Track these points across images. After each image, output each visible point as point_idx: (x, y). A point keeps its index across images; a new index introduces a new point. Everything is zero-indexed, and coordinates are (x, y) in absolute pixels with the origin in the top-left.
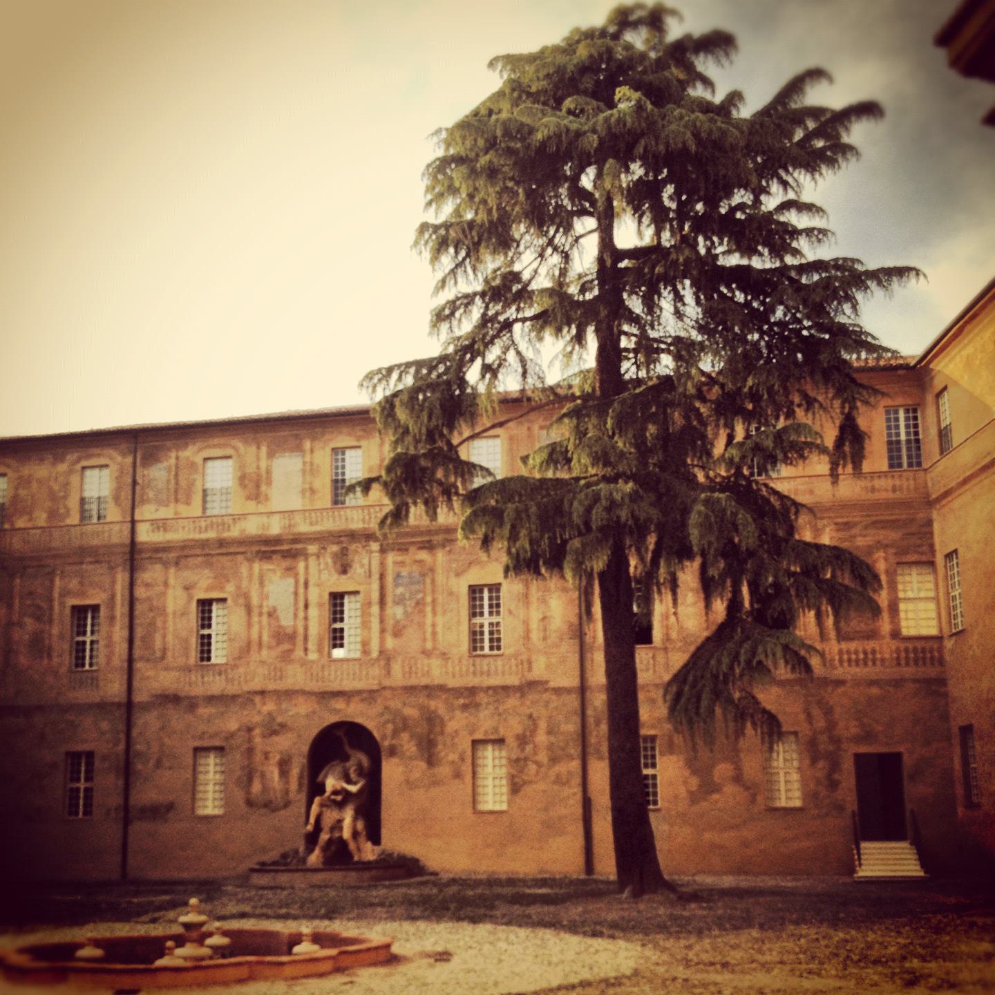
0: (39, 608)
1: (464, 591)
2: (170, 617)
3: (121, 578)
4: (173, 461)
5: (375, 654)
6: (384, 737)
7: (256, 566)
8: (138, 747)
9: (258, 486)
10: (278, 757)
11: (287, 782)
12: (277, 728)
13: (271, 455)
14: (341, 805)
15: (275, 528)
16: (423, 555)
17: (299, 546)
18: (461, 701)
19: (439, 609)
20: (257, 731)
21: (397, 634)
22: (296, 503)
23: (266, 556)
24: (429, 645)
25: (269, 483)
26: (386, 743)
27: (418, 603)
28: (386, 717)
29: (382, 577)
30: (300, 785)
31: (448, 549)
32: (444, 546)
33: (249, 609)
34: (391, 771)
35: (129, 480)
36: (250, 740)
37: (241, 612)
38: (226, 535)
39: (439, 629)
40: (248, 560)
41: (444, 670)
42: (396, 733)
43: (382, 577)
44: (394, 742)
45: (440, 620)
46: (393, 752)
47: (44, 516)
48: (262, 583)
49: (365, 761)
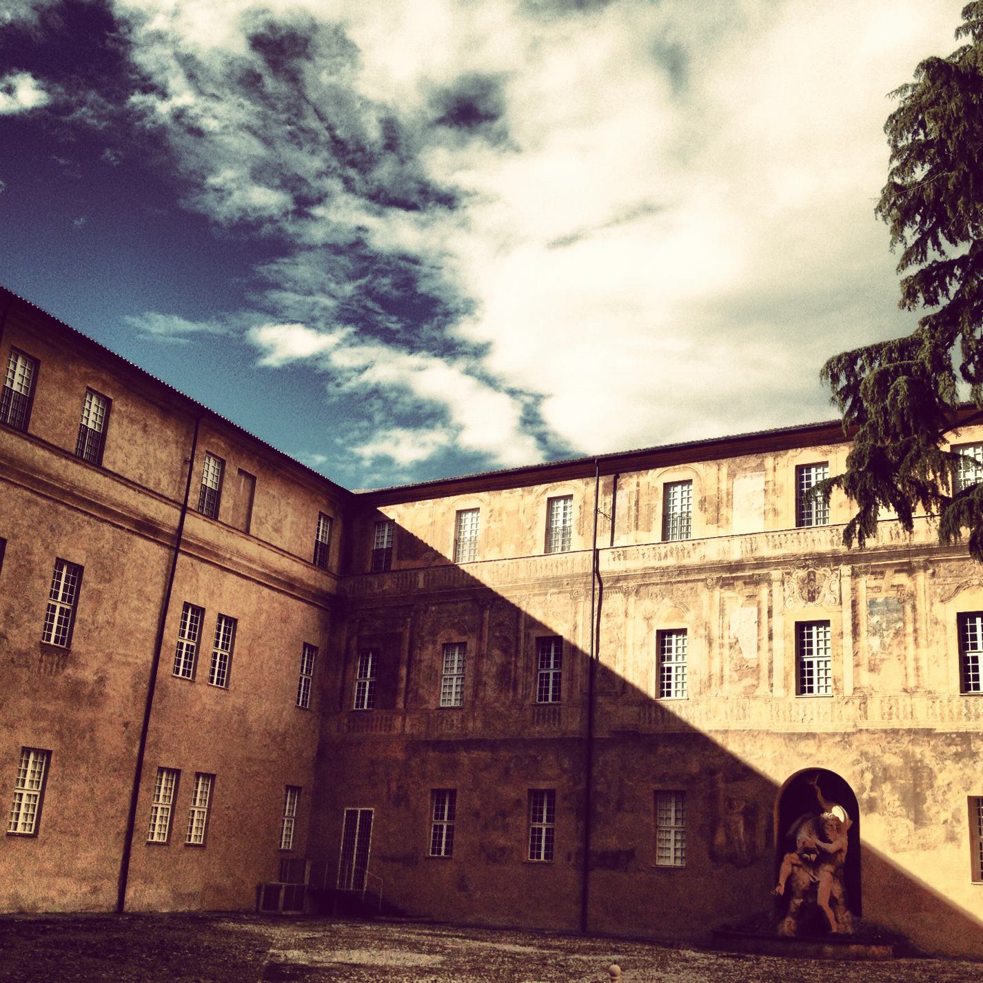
0: (506, 639)
1: (953, 620)
2: (630, 649)
3: (585, 607)
4: (634, 488)
5: (848, 691)
6: (862, 789)
7: (717, 592)
8: (599, 787)
9: (718, 509)
13: (732, 475)
14: (815, 866)
15: (736, 553)
16: (902, 579)
17: (764, 571)
18: (953, 749)
19: (922, 641)
20: (720, 775)
21: (872, 669)
22: (758, 525)
23: (726, 583)
24: (912, 683)
25: (730, 504)
26: (865, 796)
27: (897, 633)
28: (865, 764)
29: (854, 604)
31: (931, 571)
32: (926, 569)
33: (710, 644)
35: (593, 509)
37: (703, 643)
38: (686, 562)
39: (923, 663)
40: (707, 586)
41: (931, 711)
42: (875, 784)
43: (854, 604)
44: (873, 794)
45: (923, 653)
46: (872, 806)
47: (513, 547)
48: (722, 611)
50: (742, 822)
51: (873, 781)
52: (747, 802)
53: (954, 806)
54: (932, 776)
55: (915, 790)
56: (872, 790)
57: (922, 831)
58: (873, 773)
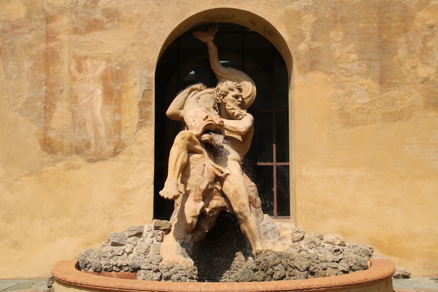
10: (100, 70)
11: (119, 111)
12: (98, 15)
20: (64, 21)
26: (302, 47)
30: (143, 116)
36: (50, 37)
42: (319, 29)
44: (316, 45)
46: (313, 65)
49: (249, 88)
50: (99, 92)
52: (109, 61)
54: (407, 17)
56: (313, 40)
57: (395, 93)
58: (316, 14)
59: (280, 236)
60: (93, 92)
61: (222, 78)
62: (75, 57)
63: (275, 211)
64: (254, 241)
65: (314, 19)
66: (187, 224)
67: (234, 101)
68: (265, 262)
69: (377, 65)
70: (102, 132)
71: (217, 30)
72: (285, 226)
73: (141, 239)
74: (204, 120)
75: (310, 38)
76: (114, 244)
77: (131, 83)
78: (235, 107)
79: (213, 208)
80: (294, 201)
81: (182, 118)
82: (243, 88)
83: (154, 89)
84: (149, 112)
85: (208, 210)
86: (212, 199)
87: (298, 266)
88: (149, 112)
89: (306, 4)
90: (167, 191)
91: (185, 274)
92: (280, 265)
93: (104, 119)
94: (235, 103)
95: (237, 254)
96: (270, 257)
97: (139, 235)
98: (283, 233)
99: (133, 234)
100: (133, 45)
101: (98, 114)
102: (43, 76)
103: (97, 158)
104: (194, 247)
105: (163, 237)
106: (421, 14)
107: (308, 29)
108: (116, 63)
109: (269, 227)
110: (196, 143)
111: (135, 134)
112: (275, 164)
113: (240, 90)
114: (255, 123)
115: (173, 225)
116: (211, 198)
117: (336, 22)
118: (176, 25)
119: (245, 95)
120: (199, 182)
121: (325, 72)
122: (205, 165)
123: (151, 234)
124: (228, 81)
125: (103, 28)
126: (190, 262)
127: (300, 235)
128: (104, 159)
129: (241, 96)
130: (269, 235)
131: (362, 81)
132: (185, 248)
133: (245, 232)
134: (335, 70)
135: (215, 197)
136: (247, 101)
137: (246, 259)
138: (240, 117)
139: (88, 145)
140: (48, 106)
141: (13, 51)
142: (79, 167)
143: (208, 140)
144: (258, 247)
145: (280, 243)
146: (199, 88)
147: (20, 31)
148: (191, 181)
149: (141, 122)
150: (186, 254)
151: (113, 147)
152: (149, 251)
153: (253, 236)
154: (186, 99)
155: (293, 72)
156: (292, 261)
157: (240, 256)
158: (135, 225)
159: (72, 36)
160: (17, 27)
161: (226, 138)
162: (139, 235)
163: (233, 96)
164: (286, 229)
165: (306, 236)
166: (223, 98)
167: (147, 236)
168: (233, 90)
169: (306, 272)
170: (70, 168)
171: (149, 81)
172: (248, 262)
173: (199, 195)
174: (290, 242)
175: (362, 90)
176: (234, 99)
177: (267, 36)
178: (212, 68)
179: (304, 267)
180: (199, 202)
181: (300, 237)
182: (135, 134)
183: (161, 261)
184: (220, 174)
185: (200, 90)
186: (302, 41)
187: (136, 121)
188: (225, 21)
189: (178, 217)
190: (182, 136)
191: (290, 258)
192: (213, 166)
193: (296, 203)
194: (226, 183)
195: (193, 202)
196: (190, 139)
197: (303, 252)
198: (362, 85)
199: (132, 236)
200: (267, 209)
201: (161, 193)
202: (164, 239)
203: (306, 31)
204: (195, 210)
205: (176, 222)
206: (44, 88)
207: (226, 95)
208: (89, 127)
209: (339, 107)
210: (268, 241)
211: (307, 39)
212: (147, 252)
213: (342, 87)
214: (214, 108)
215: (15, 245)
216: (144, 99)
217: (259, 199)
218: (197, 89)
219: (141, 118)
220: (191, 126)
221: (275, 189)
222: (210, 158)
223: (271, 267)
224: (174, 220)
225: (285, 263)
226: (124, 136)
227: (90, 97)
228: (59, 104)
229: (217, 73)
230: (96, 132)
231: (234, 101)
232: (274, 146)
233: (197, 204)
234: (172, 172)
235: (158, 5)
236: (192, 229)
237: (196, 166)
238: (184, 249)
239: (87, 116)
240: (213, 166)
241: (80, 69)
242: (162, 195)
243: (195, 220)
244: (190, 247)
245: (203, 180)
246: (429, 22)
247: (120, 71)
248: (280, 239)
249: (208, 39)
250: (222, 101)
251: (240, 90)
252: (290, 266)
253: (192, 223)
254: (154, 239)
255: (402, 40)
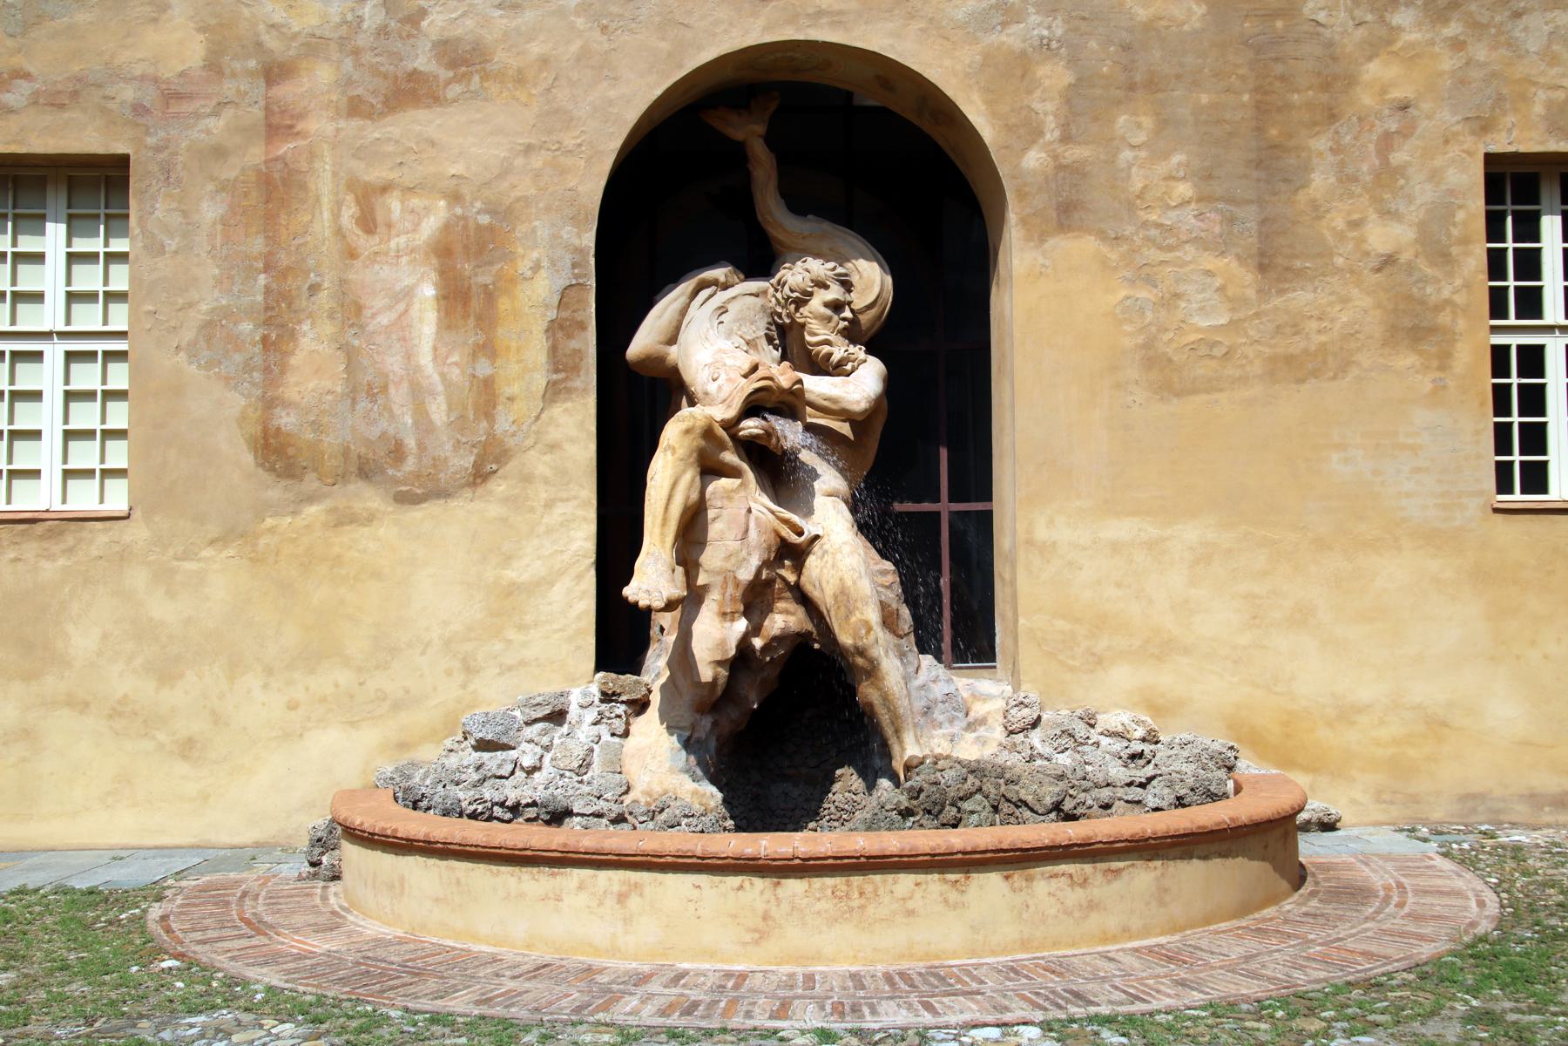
10: (430, 226)
11: (487, 349)
12: (423, 61)
20: (322, 76)
26: (1034, 159)
30: (561, 363)
34: (1046, 306)
36: (278, 125)
42: (1085, 107)
44: (1074, 153)
46: (1066, 214)
49: (871, 280)
50: (428, 291)
51: (1070, 96)
52: (455, 198)
53: (1425, 194)
54: (1335, 80)
55: (1260, 130)
56: (1066, 139)
57: (1301, 298)
58: (1073, 61)
59: (970, 719)
60: (409, 293)
61: (790, 249)
62: (352, 185)
63: (946, 645)
64: (897, 731)
65: (1068, 78)
66: (699, 684)
67: (829, 319)
68: (934, 789)
69: (1249, 216)
70: (438, 411)
71: (773, 106)
72: (985, 691)
73: (565, 729)
74: (745, 376)
75: (1057, 133)
76: (483, 746)
77: (524, 267)
78: (832, 337)
79: (775, 638)
80: (1009, 614)
81: (675, 372)
82: (855, 279)
83: (592, 282)
84: (578, 353)
85: (758, 643)
86: (772, 611)
87: (1029, 799)
88: (578, 353)
89: (1045, 33)
90: (644, 587)
91: (699, 828)
92: (978, 797)
93: (443, 376)
94: (832, 324)
95: (838, 772)
96: (950, 775)
97: (558, 717)
98: (978, 710)
99: (540, 715)
100: (528, 149)
101: (425, 359)
102: (258, 244)
103: (423, 490)
104: (719, 751)
105: (628, 724)
106: (1374, 70)
107: (1049, 107)
108: (478, 205)
109: (939, 690)
110: (722, 447)
111: (538, 418)
112: (945, 507)
113: (847, 285)
114: (892, 383)
115: (656, 688)
116: (769, 609)
117: (1132, 87)
118: (659, 92)
119: (860, 300)
120: (733, 560)
121: (1102, 235)
122: (749, 511)
123: (591, 715)
124: (810, 259)
125: (436, 100)
126: (712, 795)
127: (1028, 714)
128: (442, 493)
129: (849, 303)
130: (938, 715)
131: (1210, 262)
132: (695, 753)
133: (871, 705)
134: (1129, 230)
135: (780, 605)
136: (864, 319)
137: (871, 787)
138: (849, 367)
139: (397, 453)
140: (274, 336)
141: (167, 170)
142: (370, 519)
143: (757, 436)
144: (909, 748)
145: (970, 736)
146: (722, 279)
147: (187, 107)
148: (712, 559)
149: (555, 383)
150: (699, 772)
151: (472, 459)
152: (589, 765)
153: (896, 720)
154: (683, 312)
155: (1006, 235)
156: (1011, 787)
157: (848, 781)
158: (545, 688)
159: (342, 124)
160: (179, 96)
161: (809, 428)
162: (558, 717)
163: (826, 305)
164: (986, 698)
165: (1045, 717)
166: (797, 310)
167: (579, 722)
168: (826, 287)
169: (1053, 815)
170: (343, 519)
171: (577, 258)
172: (875, 794)
173: (733, 599)
174: (998, 734)
175: (1208, 290)
176: (828, 312)
177: (926, 125)
178: (760, 218)
179: (1048, 801)
180: (733, 620)
181: (1029, 720)
182: (538, 418)
183: (626, 792)
184: (794, 538)
185: (725, 287)
186: (1034, 142)
187: (540, 381)
188: (800, 78)
189: (669, 664)
190: (684, 426)
191: (1007, 776)
192: (773, 512)
193: (1016, 621)
194: (812, 562)
195: (717, 621)
196: (708, 433)
197: (1039, 762)
198: (1209, 273)
199: (536, 721)
200: (926, 642)
201: (630, 592)
202: (632, 729)
203: (1046, 114)
204: (722, 643)
205: (663, 680)
206: (262, 279)
207: (806, 302)
208: (399, 396)
209: (1140, 340)
210: (935, 733)
211: (1048, 136)
212: (585, 765)
213: (1150, 281)
214: (770, 340)
215: (188, 748)
216: (564, 314)
217: (905, 612)
218: (715, 283)
219: (557, 371)
220: (706, 394)
221: (945, 582)
222: (764, 489)
223: (952, 805)
224: (658, 675)
225: (993, 791)
226: (503, 424)
227: (401, 307)
228: (305, 327)
229: (774, 232)
230: (421, 412)
231: (829, 319)
232: (944, 453)
233: (728, 624)
234: (657, 530)
235: (604, 29)
236: (714, 699)
237: (724, 512)
238: (692, 758)
239: (393, 363)
240: (773, 512)
241: (368, 223)
242: (631, 599)
243: (724, 673)
244: (708, 751)
245: (744, 553)
246: (1397, 94)
247: (490, 228)
248: (970, 727)
249: (750, 132)
250: (793, 320)
251: (847, 285)
252: (1008, 801)
253: (715, 679)
254: (603, 730)
255: (1321, 143)
